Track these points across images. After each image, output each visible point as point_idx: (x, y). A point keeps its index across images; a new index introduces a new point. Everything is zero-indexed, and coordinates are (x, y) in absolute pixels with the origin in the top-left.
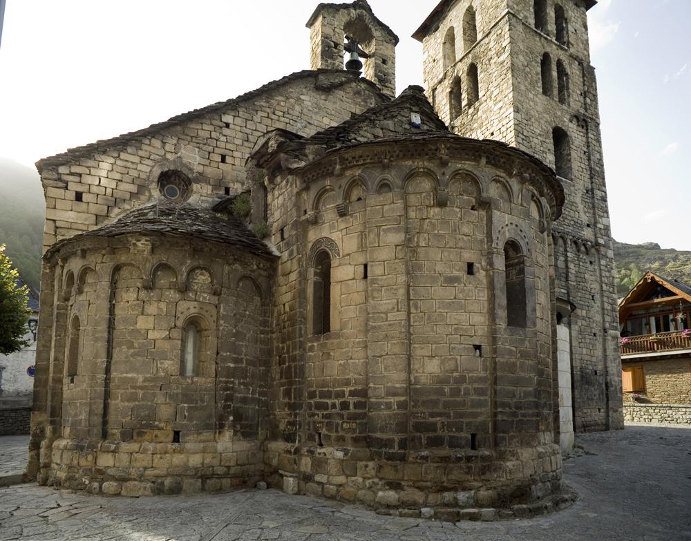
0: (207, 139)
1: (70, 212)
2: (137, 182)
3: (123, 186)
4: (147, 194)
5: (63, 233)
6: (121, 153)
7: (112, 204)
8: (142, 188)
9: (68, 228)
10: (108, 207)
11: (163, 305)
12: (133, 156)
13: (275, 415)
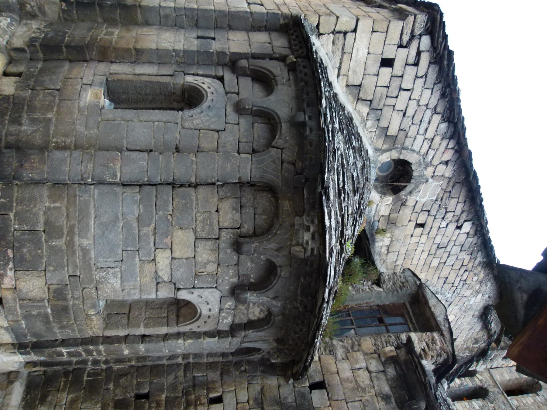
0: (446, 208)
1: (366, 51)
2: (402, 135)
3: (397, 118)
4: (385, 147)
5: (337, 42)
6: (440, 116)
7: (375, 105)
8: (392, 141)
9: (343, 49)
10: (371, 101)
11: (211, 268)
12: (435, 130)
13: (63, 390)
